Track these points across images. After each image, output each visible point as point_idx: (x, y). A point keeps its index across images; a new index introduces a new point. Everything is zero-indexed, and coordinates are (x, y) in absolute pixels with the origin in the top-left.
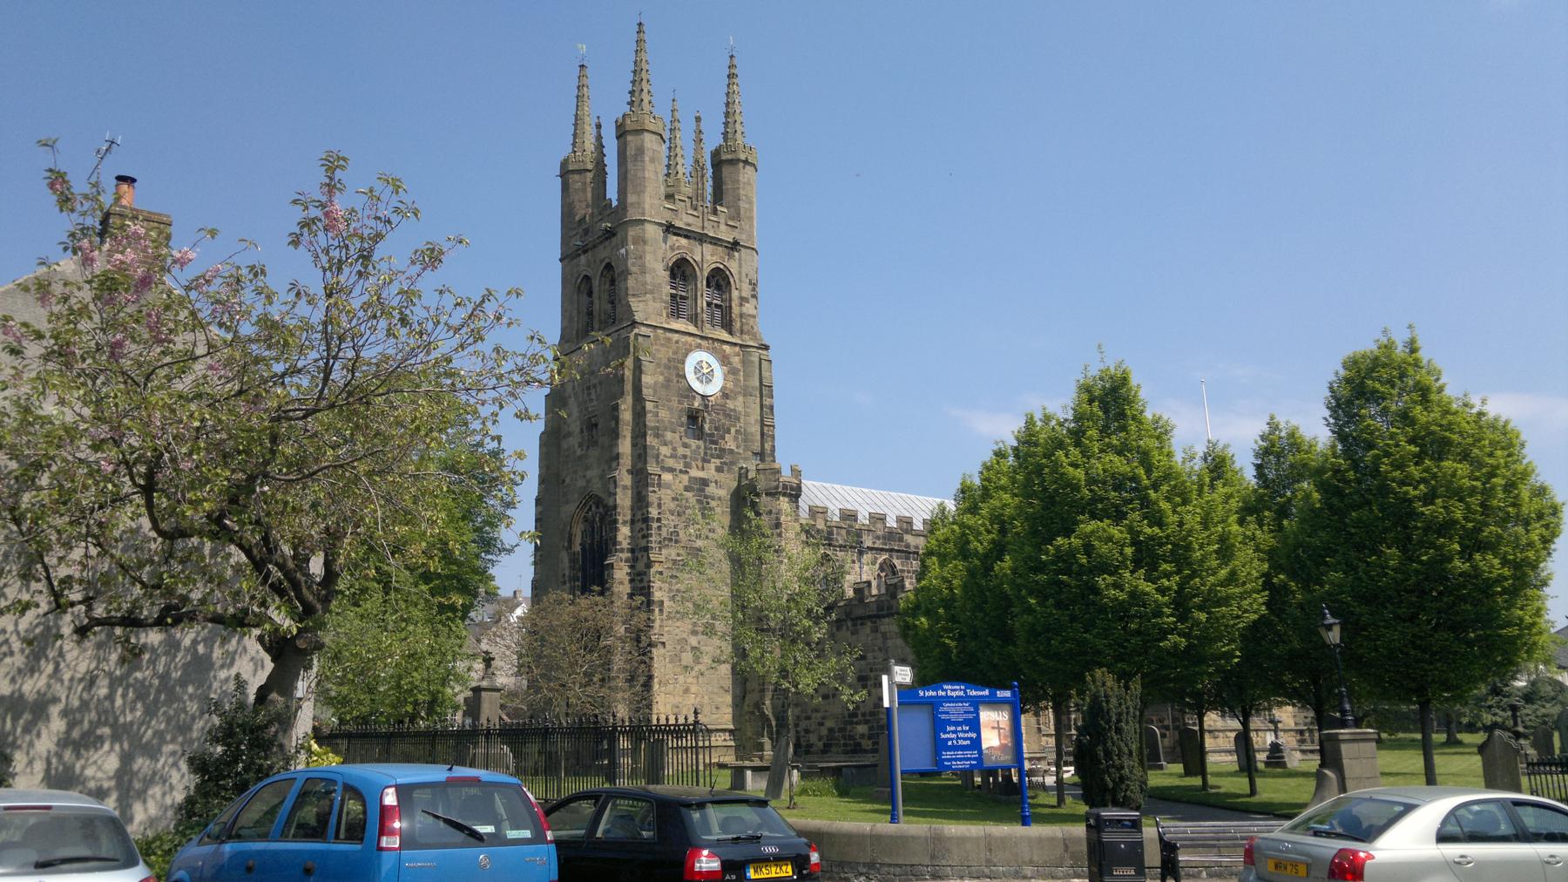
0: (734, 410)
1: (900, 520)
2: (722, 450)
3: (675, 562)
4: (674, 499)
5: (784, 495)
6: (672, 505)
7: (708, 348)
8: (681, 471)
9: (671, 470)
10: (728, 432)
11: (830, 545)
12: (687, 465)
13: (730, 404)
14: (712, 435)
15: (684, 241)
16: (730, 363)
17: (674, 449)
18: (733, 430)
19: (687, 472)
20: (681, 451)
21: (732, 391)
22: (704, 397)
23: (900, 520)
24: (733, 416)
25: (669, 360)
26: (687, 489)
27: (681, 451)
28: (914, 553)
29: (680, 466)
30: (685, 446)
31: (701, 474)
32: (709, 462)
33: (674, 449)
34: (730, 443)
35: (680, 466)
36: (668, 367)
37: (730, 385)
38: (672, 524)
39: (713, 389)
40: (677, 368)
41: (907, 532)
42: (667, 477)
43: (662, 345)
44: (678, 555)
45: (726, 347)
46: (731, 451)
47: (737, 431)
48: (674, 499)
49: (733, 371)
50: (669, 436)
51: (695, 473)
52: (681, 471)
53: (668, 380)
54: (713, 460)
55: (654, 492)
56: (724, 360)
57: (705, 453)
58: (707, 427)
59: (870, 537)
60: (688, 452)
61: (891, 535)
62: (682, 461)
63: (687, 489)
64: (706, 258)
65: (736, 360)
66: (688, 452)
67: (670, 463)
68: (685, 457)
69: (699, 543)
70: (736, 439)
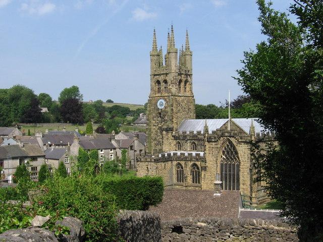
1: (197, 132)
2: (165, 120)
23: (197, 132)
24: (167, 112)
29: (157, 125)
34: (166, 118)
39: (163, 107)
41: (198, 135)
42: (155, 127)
45: (166, 97)
49: (167, 102)
50: (155, 119)
51: (159, 126)
56: (165, 100)
61: (195, 136)
64: (161, 78)
65: (168, 100)
67: (155, 124)
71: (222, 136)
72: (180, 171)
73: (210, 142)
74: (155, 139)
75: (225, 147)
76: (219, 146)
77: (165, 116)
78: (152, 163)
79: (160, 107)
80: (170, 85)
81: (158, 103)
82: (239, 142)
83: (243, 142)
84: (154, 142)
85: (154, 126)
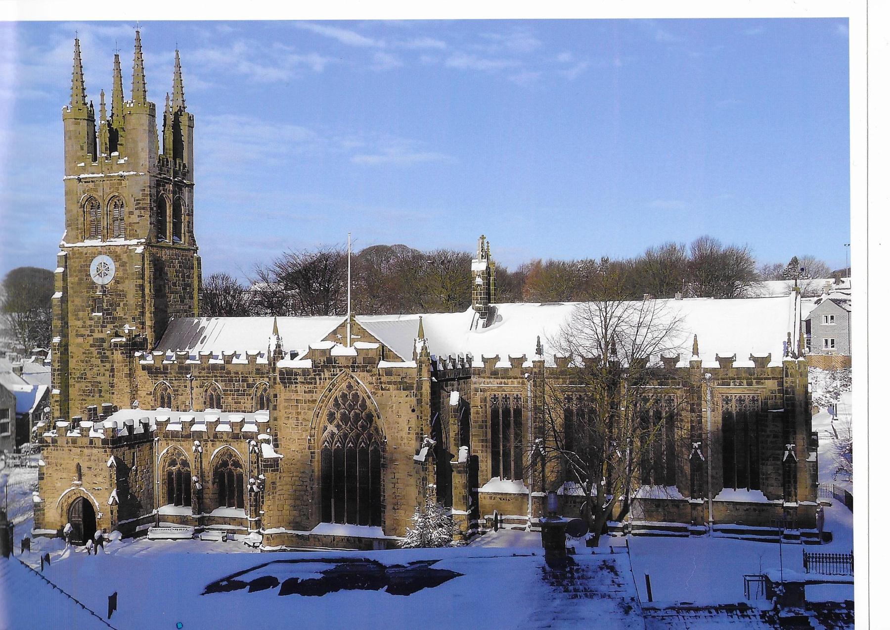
0: (123, 291)
3: (84, 391)
4: (83, 353)
5: (116, 350)
6: (83, 357)
7: (105, 253)
8: (88, 336)
9: (82, 336)
10: (119, 305)
11: (166, 377)
12: (92, 331)
13: (120, 287)
14: (108, 309)
15: (91, 185)
16: (120, 259)
17: (84, 322)
18: (121, 304)
19: (92, 335)
20: (89, 323)
21: (121, 278)
22: (102, 286)
25: (81, 267)
26: (91, 346)
27: (89, 323)
28: (235, 377)
29: (88, 333)
30: (91, 319)
31: (101, 336)
32: (106, 327)
33: (84, 322)
34: (119, 312)
35: (88, 333)
36: (80, 271)
37: (121, 274)
38: (83, 368)
39: (107, 280)
40: (86, 271)
42: (80, 340)
43: (77, 258)
44: (86, 387)
46: (121, 318)
47: (124, 304)
48: (83, 353)
49: (123, 265)
50: (81, 314)
51: (97, 335)
52: (88, 336)
53: (81, 279)
54: (108, 325)
55: (56, 353)
57: (104, 322)
58: (105, 305)
59: (197, 369)
60: (92, 323)
62: (89, 329)
63: (91, 346)
66: (92, 323)
67: (82, 331)
68: (91, 326)
69: (99, 379)
70: (123, 309)
71: (327, 367)
72: (179, 472)
73: (292, 383)
74: (83, 377)
75: (336, 400)
76: (318, 396)
77: (114, 305)
78: (95, 451)
79: (98, 281)
80: (131, 213)
81: (93, 271)
82: (381, 383)
83: (395, 383)
84: (77, 385)
85: (77, 336)
